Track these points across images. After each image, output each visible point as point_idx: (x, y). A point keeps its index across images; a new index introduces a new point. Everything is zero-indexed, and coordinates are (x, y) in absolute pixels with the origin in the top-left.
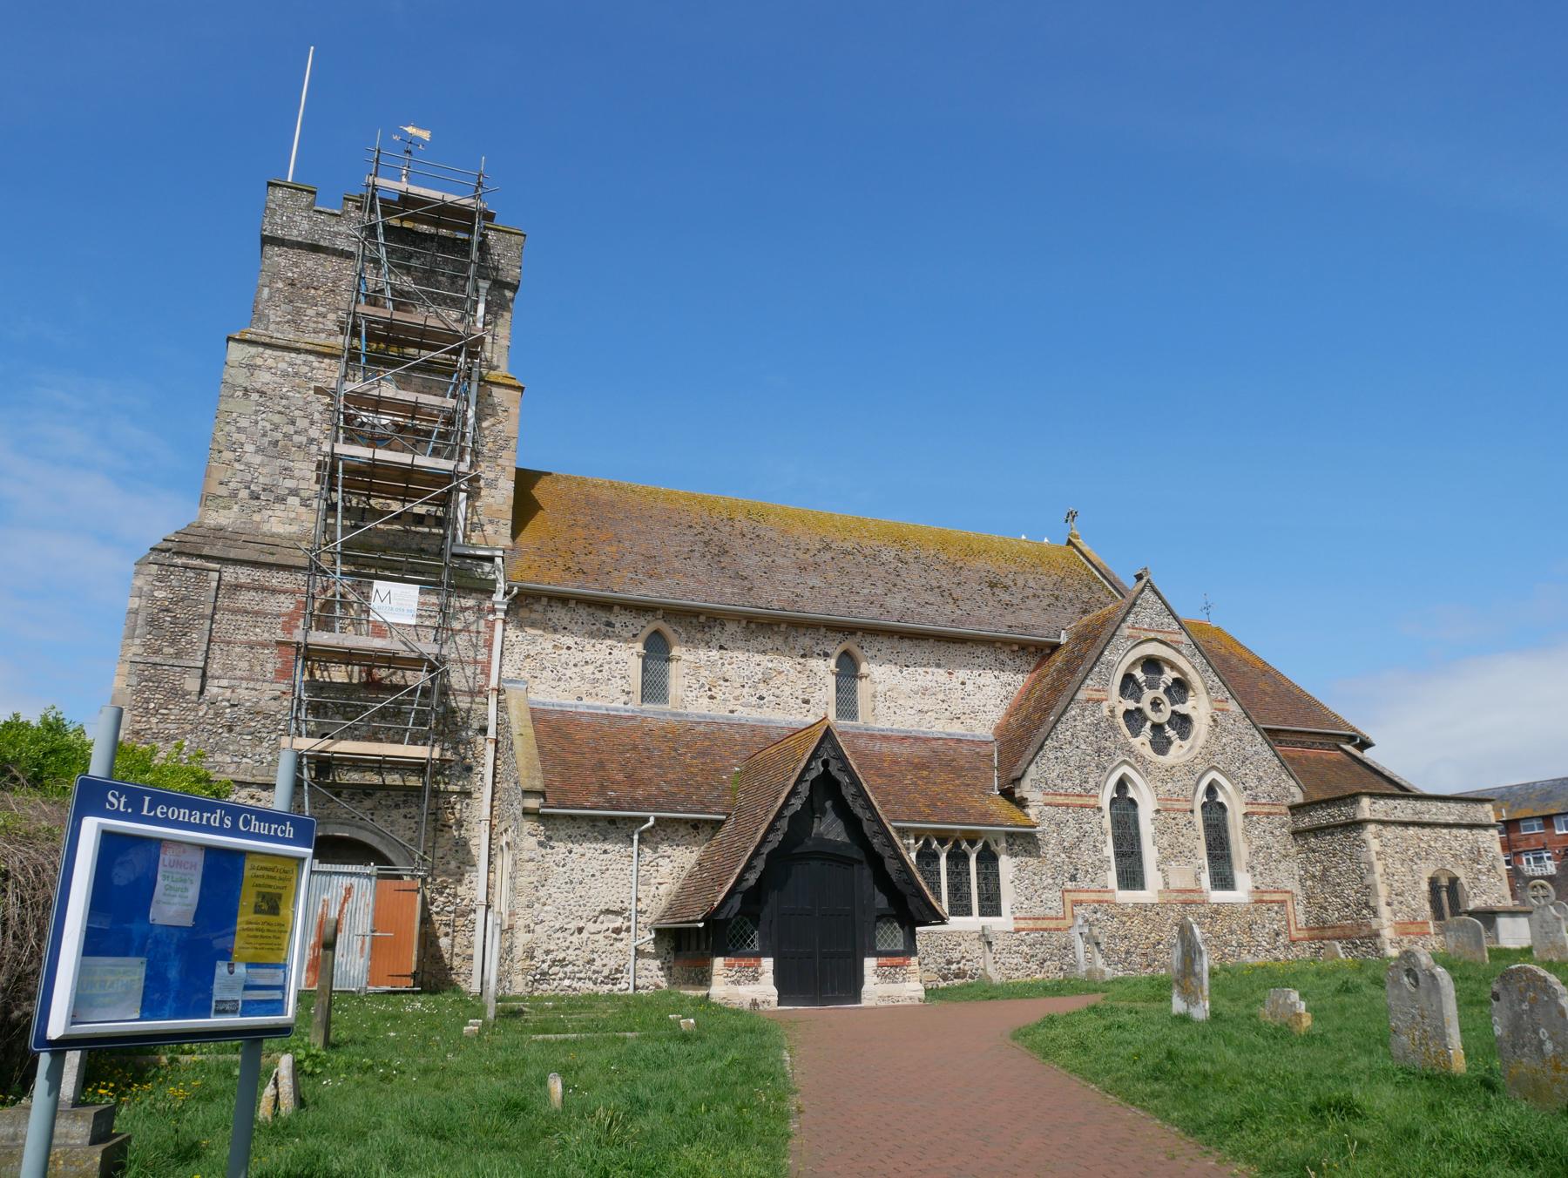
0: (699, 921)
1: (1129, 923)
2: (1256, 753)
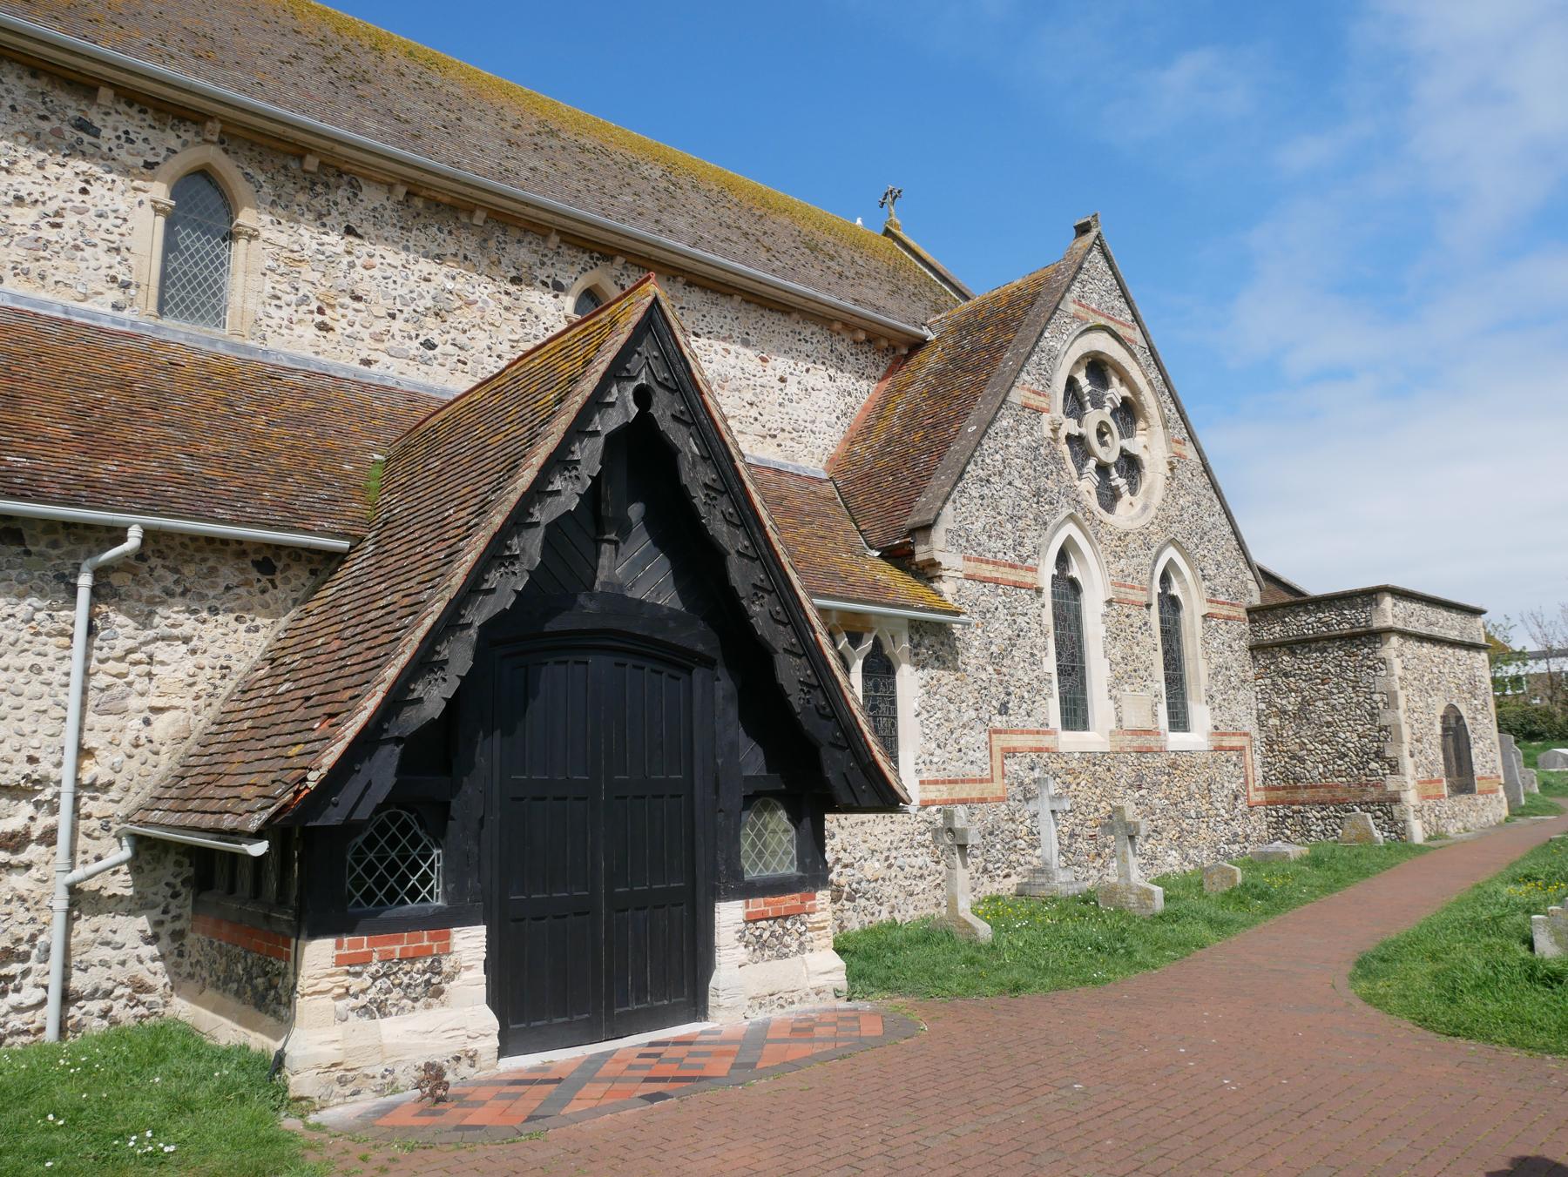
0: (258, 836)
1: (1074, 786)
2: (1214, 527)
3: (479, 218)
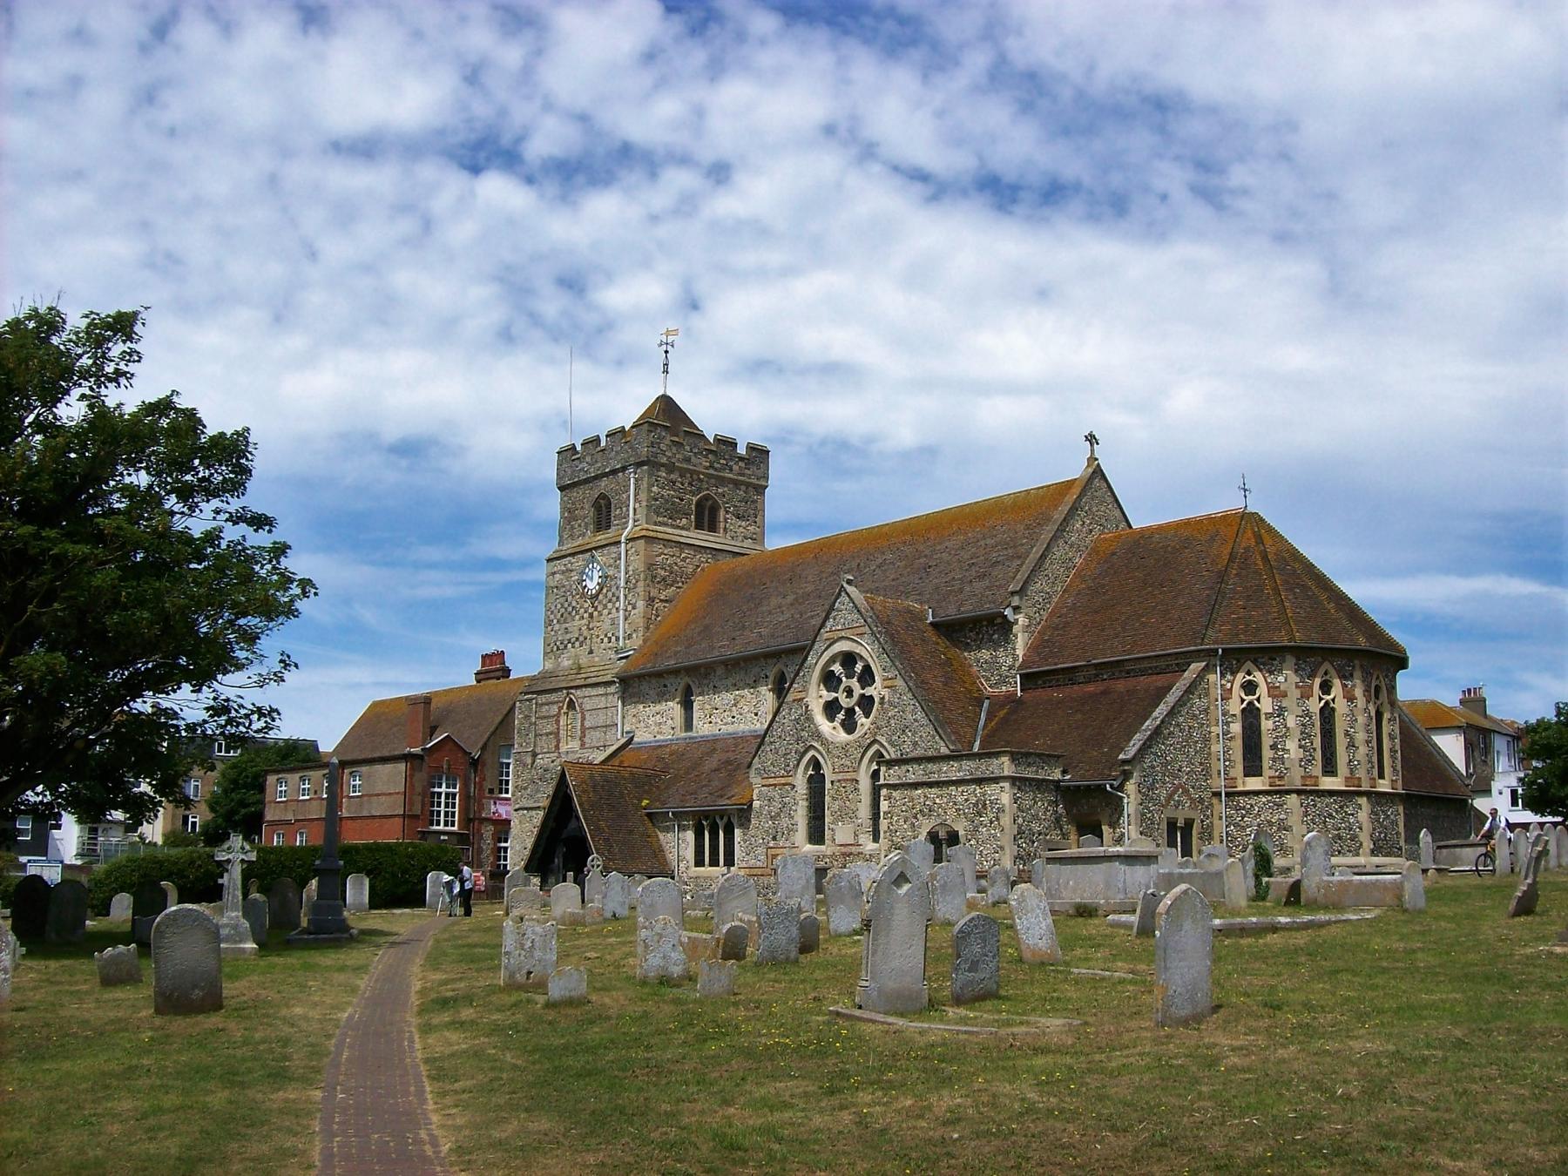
3: (742, 664)
